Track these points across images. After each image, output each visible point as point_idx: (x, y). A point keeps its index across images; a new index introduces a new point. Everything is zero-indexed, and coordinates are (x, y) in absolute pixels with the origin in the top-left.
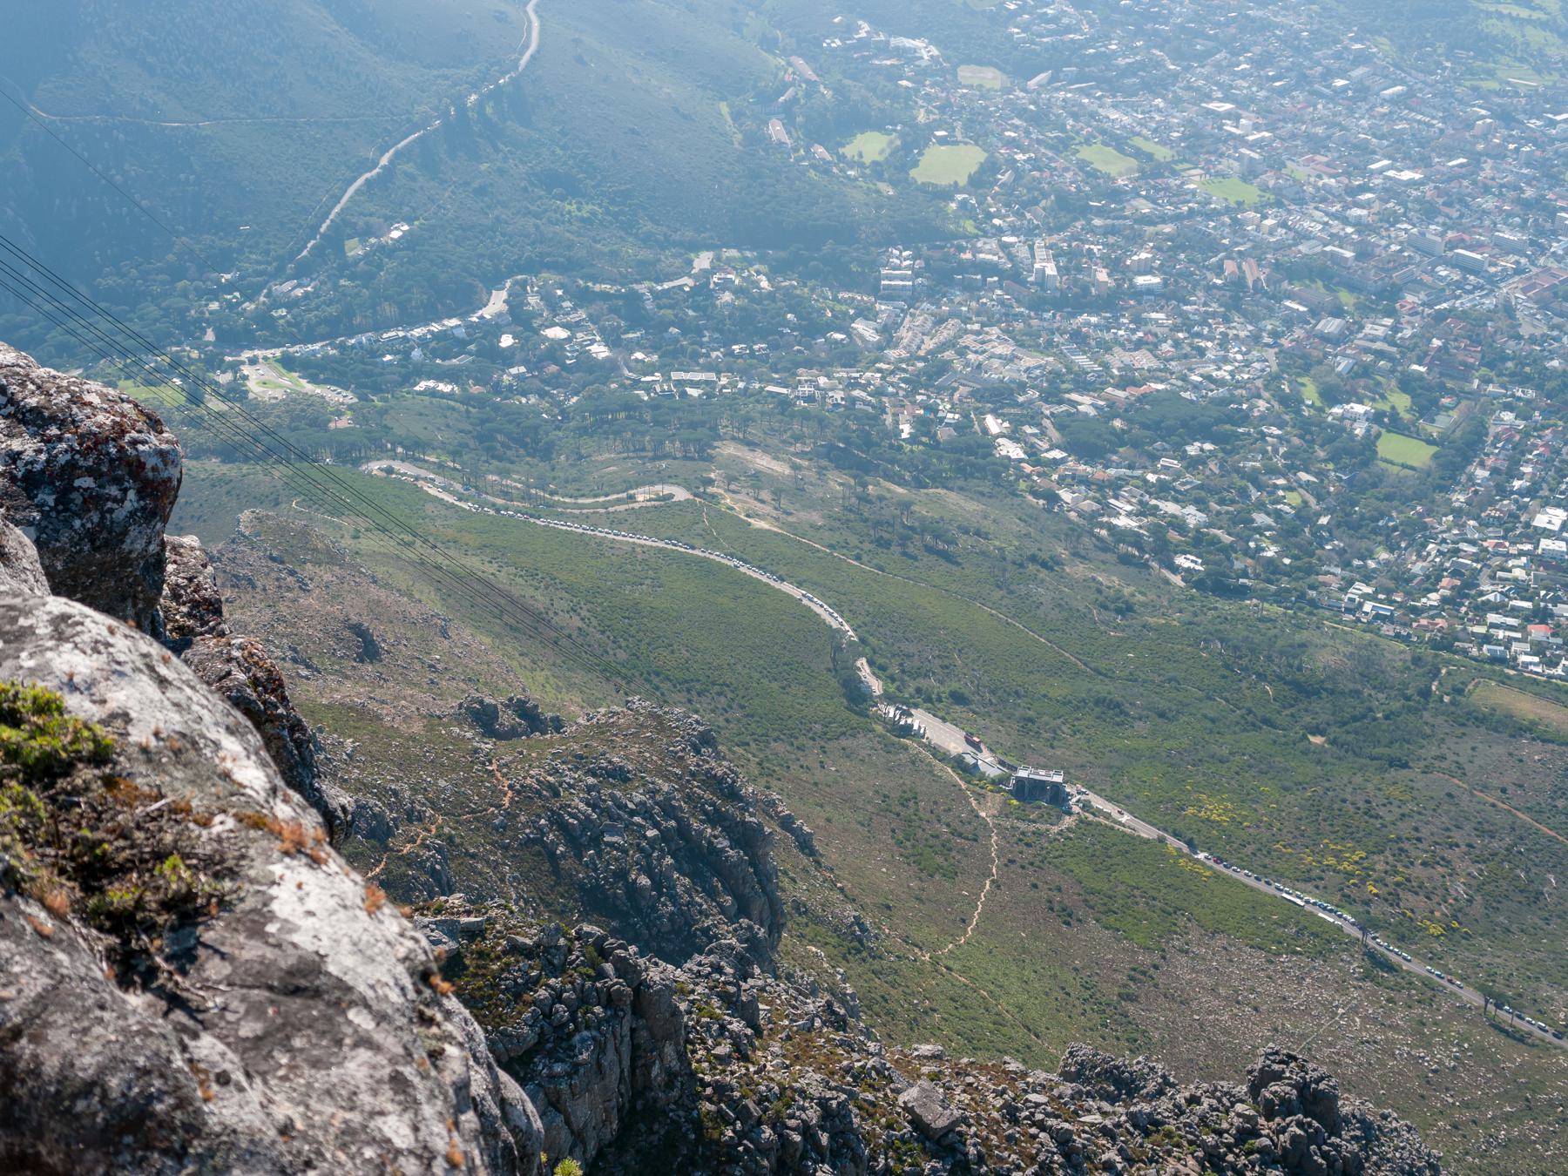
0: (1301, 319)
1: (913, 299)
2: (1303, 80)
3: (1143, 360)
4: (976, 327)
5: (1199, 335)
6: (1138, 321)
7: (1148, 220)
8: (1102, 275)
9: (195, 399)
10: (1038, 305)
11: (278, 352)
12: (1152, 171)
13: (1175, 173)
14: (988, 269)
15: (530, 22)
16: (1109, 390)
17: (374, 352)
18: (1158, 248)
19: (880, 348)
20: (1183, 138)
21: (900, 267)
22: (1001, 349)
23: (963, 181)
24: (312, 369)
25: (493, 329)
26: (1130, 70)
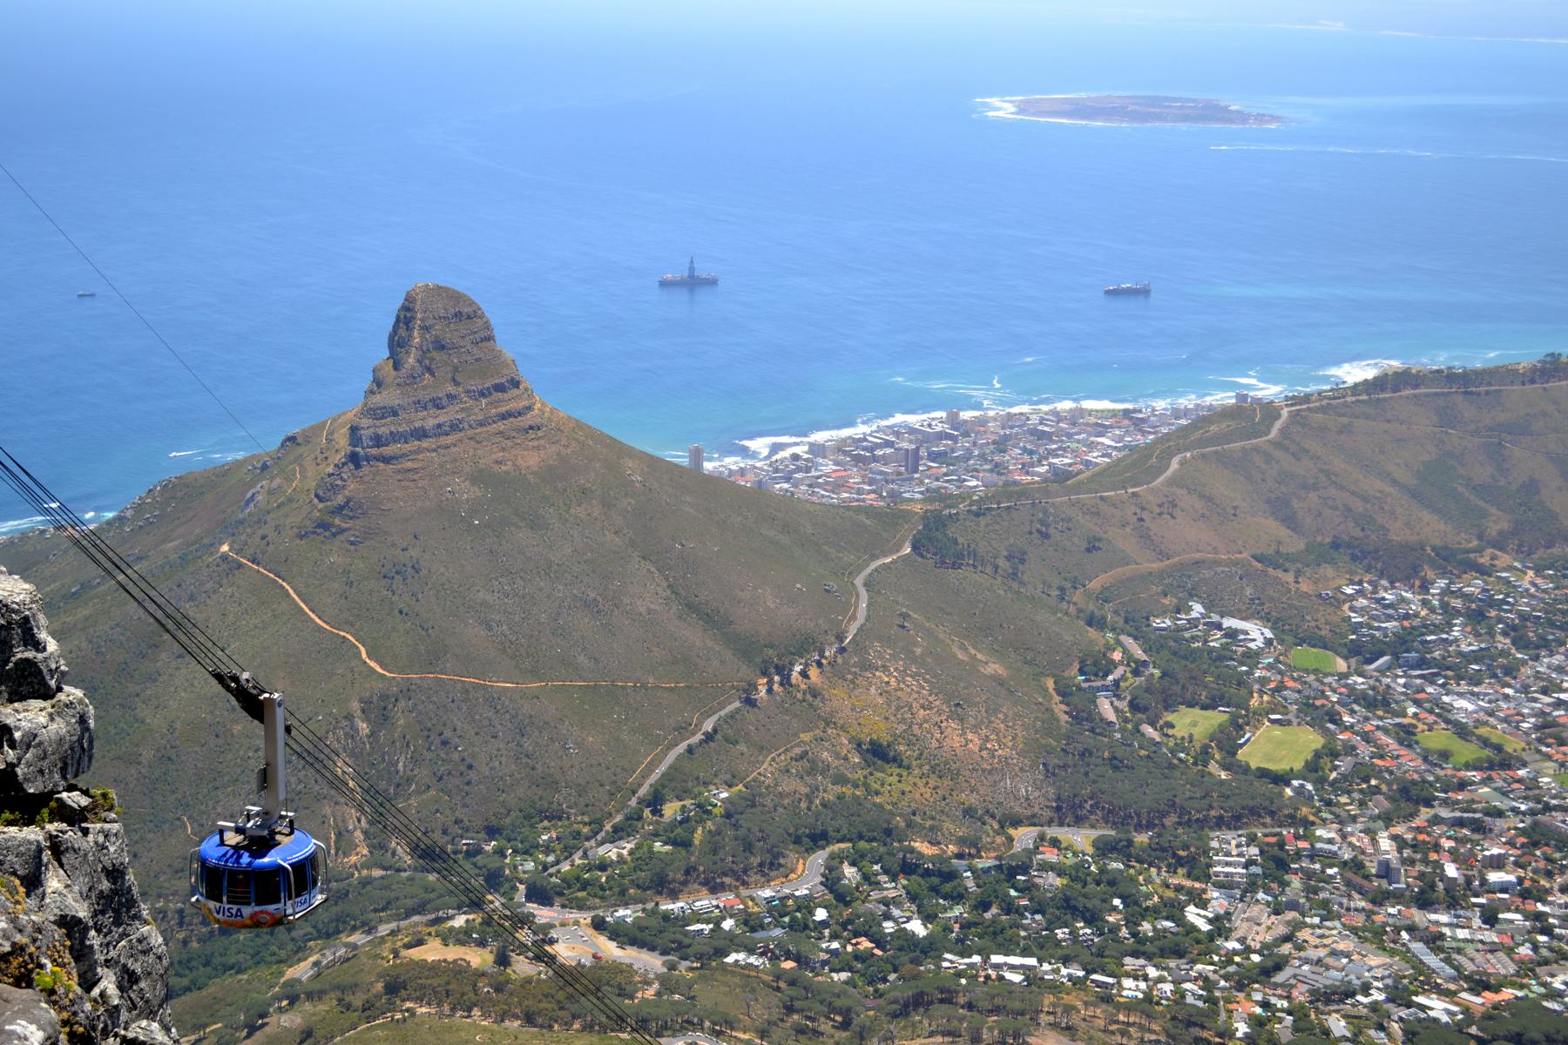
1: (1251, 886)
3: (1501, 966)
4: (1317, 920)
6: (1490, 919)
7: (1500, 814)
8: (1451, 870)
9: (503, 960)
10: (1380, 899)
12: (1499, 761)
13: (1525, 765)
14: (1330, 858)
16: (1464, 995)
18: (1511, 843)
19: (1211, 936)
20: (1537, 728)
21: (1232, 853)
22: (1341, 946)
23: (1298, 765)
24: (618, 934)
25: (807, 905)
26: (1476, 657)
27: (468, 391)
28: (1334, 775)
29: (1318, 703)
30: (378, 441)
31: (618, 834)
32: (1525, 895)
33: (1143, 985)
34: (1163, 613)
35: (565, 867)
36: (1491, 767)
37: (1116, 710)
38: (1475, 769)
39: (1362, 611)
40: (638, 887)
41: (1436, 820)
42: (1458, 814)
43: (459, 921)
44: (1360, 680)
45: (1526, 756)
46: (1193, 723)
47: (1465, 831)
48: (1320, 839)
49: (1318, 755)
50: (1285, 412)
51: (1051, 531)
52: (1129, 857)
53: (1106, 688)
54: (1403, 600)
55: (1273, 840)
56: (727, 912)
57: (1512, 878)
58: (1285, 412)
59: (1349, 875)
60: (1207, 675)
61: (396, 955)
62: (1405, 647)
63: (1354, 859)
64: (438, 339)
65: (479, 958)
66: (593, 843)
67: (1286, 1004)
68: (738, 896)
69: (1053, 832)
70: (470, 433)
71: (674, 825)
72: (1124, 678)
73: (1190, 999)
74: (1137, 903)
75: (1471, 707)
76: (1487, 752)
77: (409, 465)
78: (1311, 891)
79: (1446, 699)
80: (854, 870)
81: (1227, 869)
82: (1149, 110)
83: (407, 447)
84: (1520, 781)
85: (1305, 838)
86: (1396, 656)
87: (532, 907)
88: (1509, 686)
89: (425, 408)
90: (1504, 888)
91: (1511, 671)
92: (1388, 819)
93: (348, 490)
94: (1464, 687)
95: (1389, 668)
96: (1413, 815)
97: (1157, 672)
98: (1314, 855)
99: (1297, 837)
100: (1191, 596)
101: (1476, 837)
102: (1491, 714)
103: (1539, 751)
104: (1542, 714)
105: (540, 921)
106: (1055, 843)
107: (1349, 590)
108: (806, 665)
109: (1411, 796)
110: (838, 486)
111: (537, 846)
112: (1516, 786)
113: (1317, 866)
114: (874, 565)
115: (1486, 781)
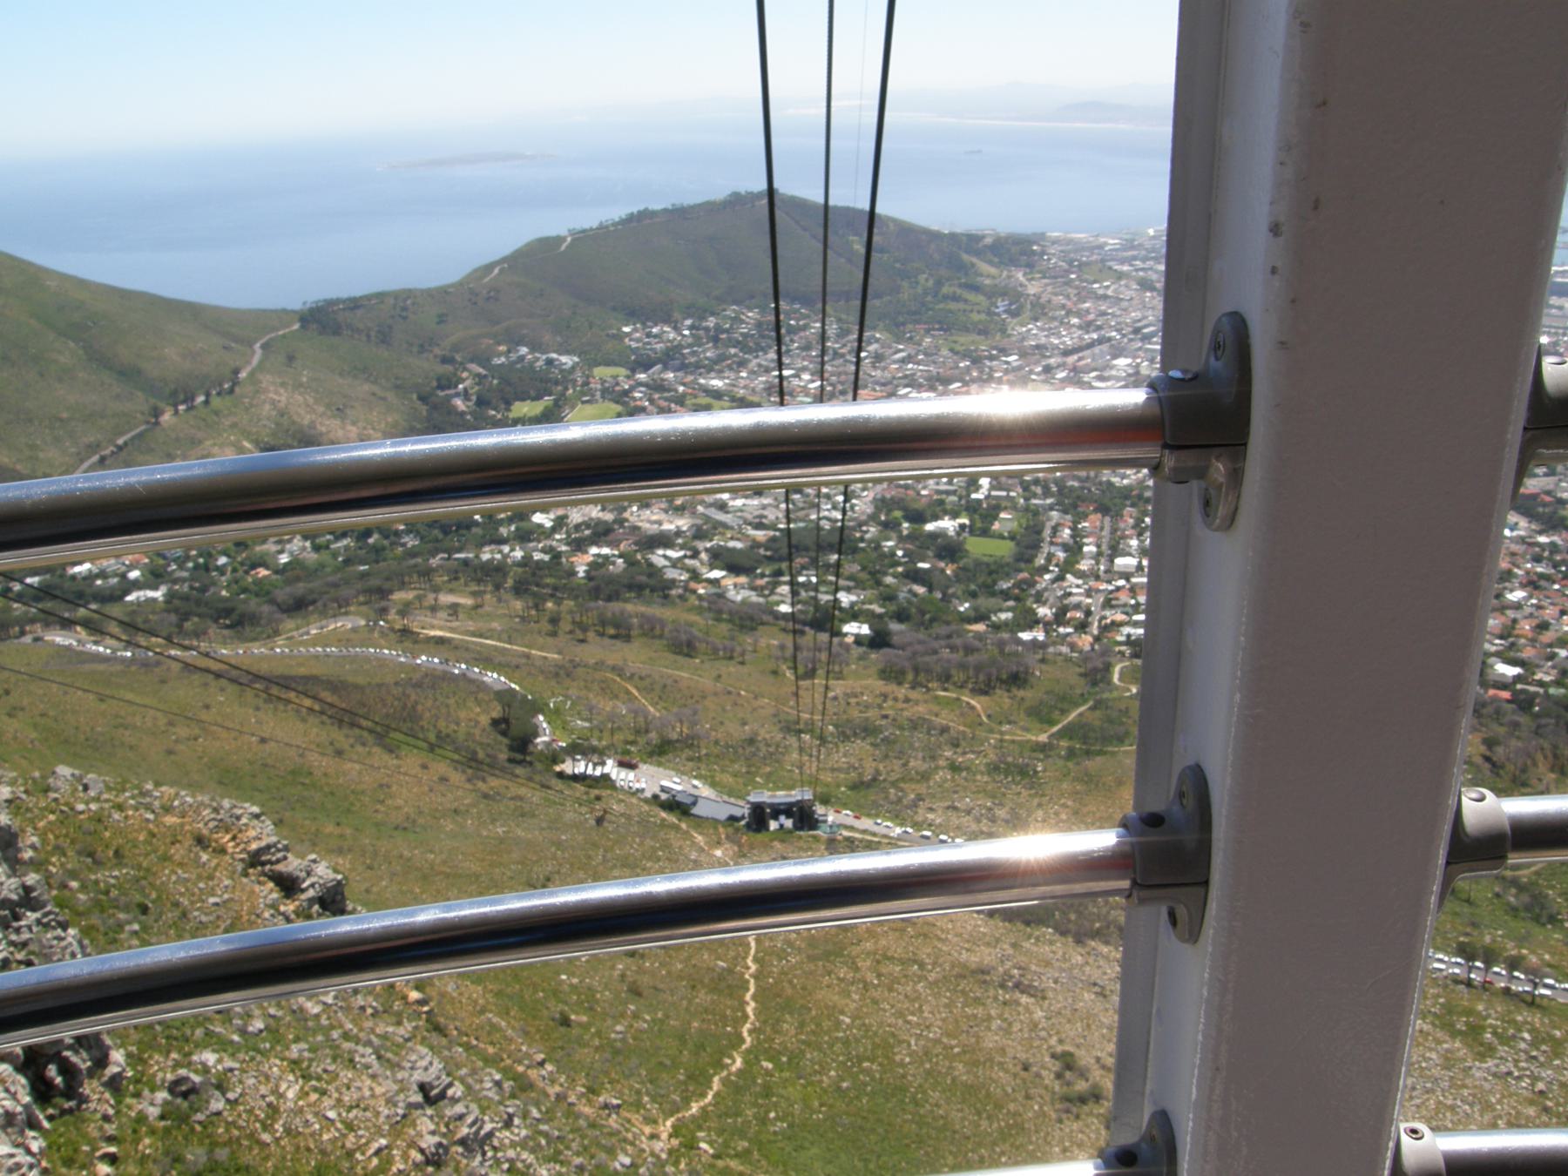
17: (90, 577)
34: (500, 355)
39: (638, 340)
62: (671, 357)
91: (742, 364)
107: (626, 329)
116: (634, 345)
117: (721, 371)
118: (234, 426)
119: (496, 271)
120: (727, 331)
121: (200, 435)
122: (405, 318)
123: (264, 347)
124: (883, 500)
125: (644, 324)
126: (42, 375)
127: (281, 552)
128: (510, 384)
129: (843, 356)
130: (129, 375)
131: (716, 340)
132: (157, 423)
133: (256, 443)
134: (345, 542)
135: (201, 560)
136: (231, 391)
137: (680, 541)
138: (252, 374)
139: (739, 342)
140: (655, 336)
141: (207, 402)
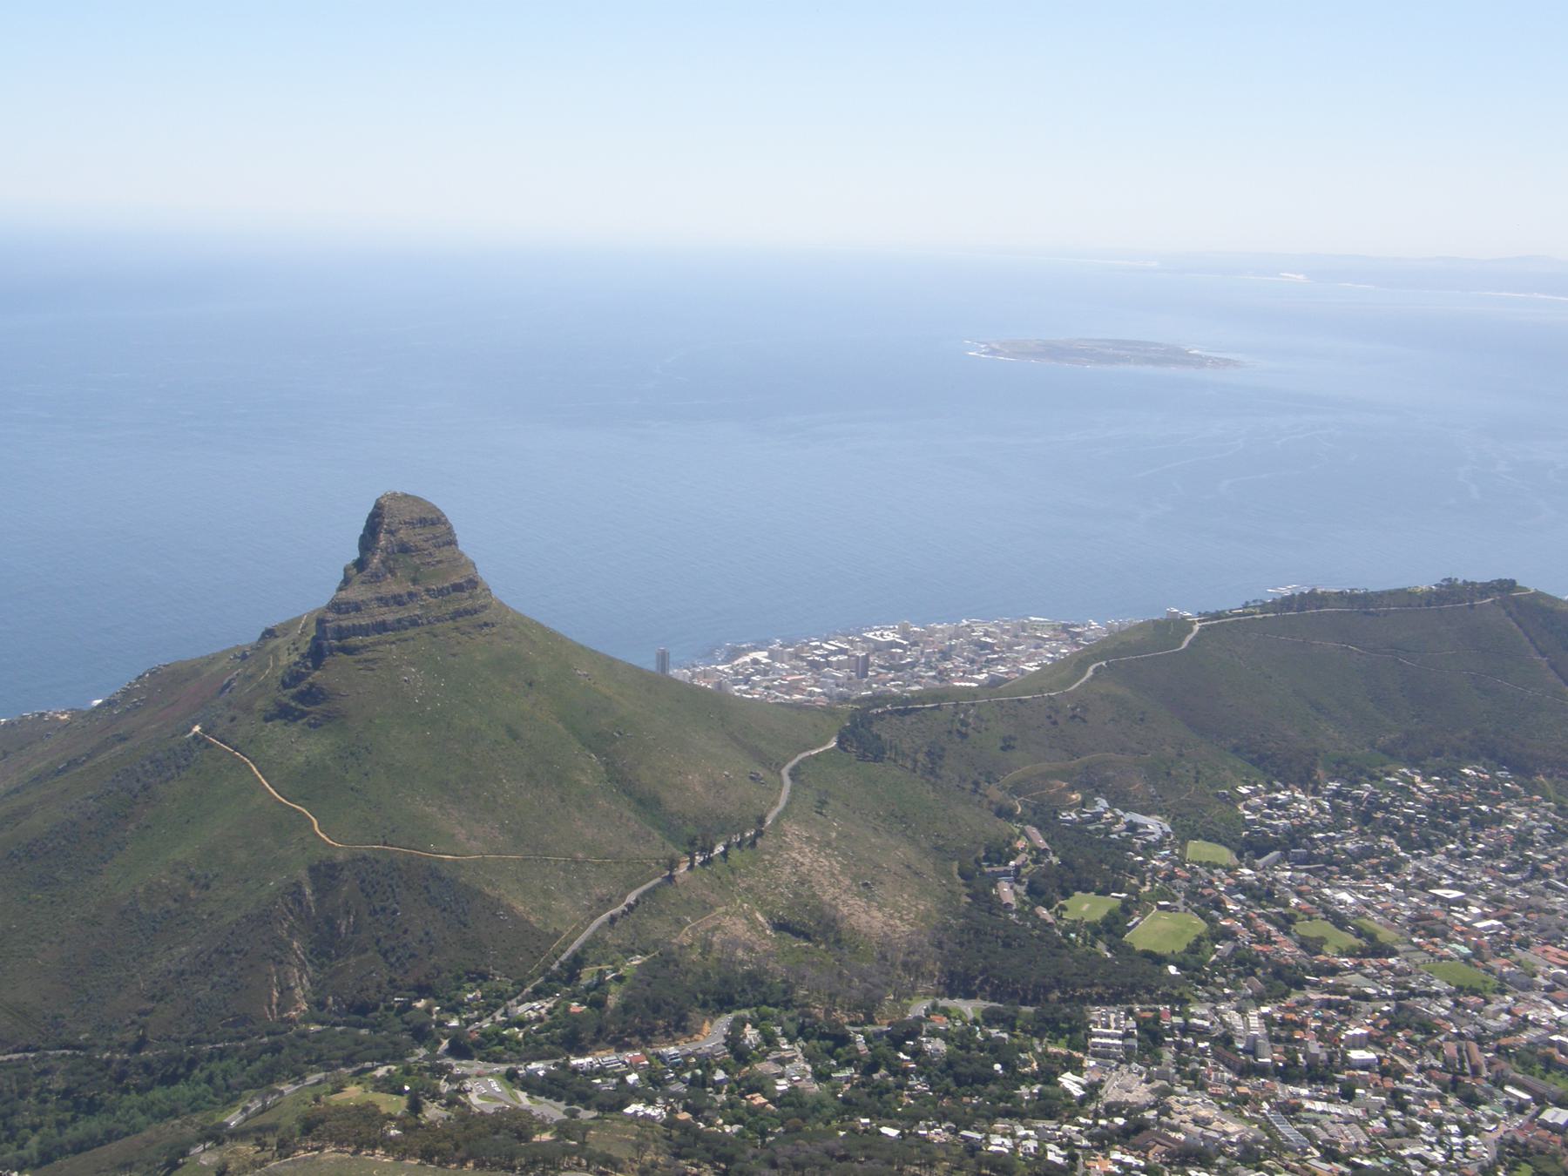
0: (1521, 1108)
2: (1537, 872)
5: (1413, 1114)
7: (1367, 998)
8: (1314, 1047)
9: (415, 1107)
10: (1246, 1071)
11: (503, 1068)
14: (1201, 1033)
15: (782, 784)
19: (1083, 1101)
21: (1110, 1025)
22: (1203, 1113)
24: (532, 1085)
25: (706, 1062)
27: (428, 590)
28: (1214, 957)
29: (1206, 892)
30: (341, 633)
31: (538, 994)
32: (1385, 1073)
33: (1008, 1142)
34: (1070, 808)
35: (486, 1024)
36: (1364, 956)
37: (1016, 894)
38: (1349, 956)
39: (1254, 810)
40: (553, 1043)
41: (1307, 1003)
42: (1326, 996)
43: (381, 1072)
44: (1247, 871)
45: (1399, 947)
46: (1087, 907)
47: (1333, 1012)
48: (1193, 1015)
49: (1199, 939)
50: (1196, 628)
51: (970, 731)
52: (1013, 1028)
53: (1007, 874)
54: (1296, 800)
55: (1149, 1015)
56: (633, 1067)
57: (1371, 1056)
58: (1196, 628)
59: (1220, 1049)
60: (1093, 861)
61: (317, 1100)
62: (1293, 843)
63: (1224, 1035)
64: (402, 544)
65: (395, 1105)
66: (514, 1002)
67: (1142, 1164)
68: (643, 1053)
69: (944, 1002)
70: (427, 628)
71: (588, 989)
72: (1024, 865)
73: (1051, 1156)
74: (1014, 1069)
75: (1350, 900)
76: (1363, 943)
77: (370, 655)
78: (1180, 1062)
79: (1327, 891)
80: (756, 1031)
81: (1104, 1041)
82: (1054, 352)
83: (369, 640)
84: (1391, 968)
85: (1179, 1014)
86: (1285, 851)
87: (449, 1061)
88: (1387, 880)
89: (387, 605)
90: (1365, 1066)
91: (1394, 866)
92: (1260, 1000)
93: (311, 673)
94: (1347, 880)
95: (1277, 863)
96: (1286, 995)
97: (1055, 860)
98: (1186, 1029)
99: (1173, 1013)
100: (1097, 793)
101: (1343, 1017)
102: (1367, 905)
103: (1411, 942)
104: (1418, 908)
105: (457, 1071)
106: (946, 1012)
107: (1244, 790)
108: (727, 847)
109: (1284, 979)
110: (793, 687)
111: (462, 1004)
112: (1386, 972)
113: (1190, 1040)
114: (800, 757)
115: (1357, 968)
116: (1249, 815)
117: (1359, 877)
118: (749, 889)
119: (1090, 673)
120: (1385, 808)
121: (713, 898)
122: (964, 736)
123: (794, 774)
124: (1513, 1143)
125: (1270, 783)
126: (563, 800)
127: (781, 1076)
128: (1073, 869)
129: (1546, 874)
130: (648, 804)
131: (1366, 818)
132: (671, 878)
133: (770, 916)
134: (848, 1072)
135: (699, 1072)
136: (753, 844)
137: (1221, 1160)
138: (777, 821)
139: (1397, 828)
140: (1282, 807)
141: (724, 854)
